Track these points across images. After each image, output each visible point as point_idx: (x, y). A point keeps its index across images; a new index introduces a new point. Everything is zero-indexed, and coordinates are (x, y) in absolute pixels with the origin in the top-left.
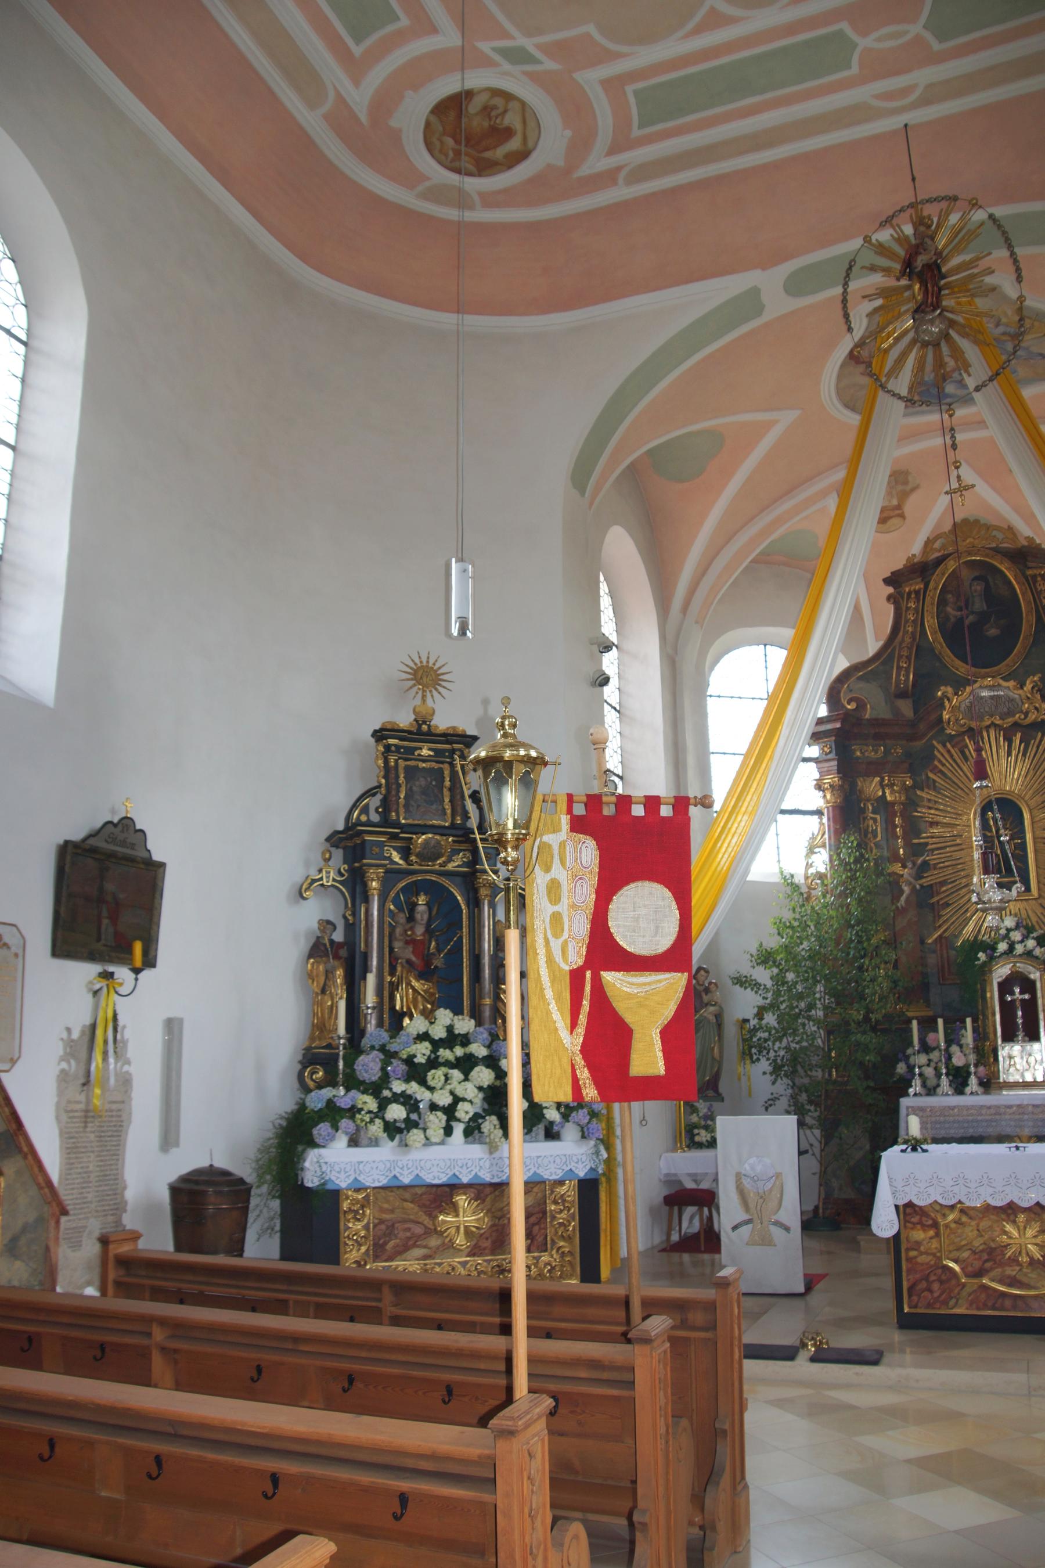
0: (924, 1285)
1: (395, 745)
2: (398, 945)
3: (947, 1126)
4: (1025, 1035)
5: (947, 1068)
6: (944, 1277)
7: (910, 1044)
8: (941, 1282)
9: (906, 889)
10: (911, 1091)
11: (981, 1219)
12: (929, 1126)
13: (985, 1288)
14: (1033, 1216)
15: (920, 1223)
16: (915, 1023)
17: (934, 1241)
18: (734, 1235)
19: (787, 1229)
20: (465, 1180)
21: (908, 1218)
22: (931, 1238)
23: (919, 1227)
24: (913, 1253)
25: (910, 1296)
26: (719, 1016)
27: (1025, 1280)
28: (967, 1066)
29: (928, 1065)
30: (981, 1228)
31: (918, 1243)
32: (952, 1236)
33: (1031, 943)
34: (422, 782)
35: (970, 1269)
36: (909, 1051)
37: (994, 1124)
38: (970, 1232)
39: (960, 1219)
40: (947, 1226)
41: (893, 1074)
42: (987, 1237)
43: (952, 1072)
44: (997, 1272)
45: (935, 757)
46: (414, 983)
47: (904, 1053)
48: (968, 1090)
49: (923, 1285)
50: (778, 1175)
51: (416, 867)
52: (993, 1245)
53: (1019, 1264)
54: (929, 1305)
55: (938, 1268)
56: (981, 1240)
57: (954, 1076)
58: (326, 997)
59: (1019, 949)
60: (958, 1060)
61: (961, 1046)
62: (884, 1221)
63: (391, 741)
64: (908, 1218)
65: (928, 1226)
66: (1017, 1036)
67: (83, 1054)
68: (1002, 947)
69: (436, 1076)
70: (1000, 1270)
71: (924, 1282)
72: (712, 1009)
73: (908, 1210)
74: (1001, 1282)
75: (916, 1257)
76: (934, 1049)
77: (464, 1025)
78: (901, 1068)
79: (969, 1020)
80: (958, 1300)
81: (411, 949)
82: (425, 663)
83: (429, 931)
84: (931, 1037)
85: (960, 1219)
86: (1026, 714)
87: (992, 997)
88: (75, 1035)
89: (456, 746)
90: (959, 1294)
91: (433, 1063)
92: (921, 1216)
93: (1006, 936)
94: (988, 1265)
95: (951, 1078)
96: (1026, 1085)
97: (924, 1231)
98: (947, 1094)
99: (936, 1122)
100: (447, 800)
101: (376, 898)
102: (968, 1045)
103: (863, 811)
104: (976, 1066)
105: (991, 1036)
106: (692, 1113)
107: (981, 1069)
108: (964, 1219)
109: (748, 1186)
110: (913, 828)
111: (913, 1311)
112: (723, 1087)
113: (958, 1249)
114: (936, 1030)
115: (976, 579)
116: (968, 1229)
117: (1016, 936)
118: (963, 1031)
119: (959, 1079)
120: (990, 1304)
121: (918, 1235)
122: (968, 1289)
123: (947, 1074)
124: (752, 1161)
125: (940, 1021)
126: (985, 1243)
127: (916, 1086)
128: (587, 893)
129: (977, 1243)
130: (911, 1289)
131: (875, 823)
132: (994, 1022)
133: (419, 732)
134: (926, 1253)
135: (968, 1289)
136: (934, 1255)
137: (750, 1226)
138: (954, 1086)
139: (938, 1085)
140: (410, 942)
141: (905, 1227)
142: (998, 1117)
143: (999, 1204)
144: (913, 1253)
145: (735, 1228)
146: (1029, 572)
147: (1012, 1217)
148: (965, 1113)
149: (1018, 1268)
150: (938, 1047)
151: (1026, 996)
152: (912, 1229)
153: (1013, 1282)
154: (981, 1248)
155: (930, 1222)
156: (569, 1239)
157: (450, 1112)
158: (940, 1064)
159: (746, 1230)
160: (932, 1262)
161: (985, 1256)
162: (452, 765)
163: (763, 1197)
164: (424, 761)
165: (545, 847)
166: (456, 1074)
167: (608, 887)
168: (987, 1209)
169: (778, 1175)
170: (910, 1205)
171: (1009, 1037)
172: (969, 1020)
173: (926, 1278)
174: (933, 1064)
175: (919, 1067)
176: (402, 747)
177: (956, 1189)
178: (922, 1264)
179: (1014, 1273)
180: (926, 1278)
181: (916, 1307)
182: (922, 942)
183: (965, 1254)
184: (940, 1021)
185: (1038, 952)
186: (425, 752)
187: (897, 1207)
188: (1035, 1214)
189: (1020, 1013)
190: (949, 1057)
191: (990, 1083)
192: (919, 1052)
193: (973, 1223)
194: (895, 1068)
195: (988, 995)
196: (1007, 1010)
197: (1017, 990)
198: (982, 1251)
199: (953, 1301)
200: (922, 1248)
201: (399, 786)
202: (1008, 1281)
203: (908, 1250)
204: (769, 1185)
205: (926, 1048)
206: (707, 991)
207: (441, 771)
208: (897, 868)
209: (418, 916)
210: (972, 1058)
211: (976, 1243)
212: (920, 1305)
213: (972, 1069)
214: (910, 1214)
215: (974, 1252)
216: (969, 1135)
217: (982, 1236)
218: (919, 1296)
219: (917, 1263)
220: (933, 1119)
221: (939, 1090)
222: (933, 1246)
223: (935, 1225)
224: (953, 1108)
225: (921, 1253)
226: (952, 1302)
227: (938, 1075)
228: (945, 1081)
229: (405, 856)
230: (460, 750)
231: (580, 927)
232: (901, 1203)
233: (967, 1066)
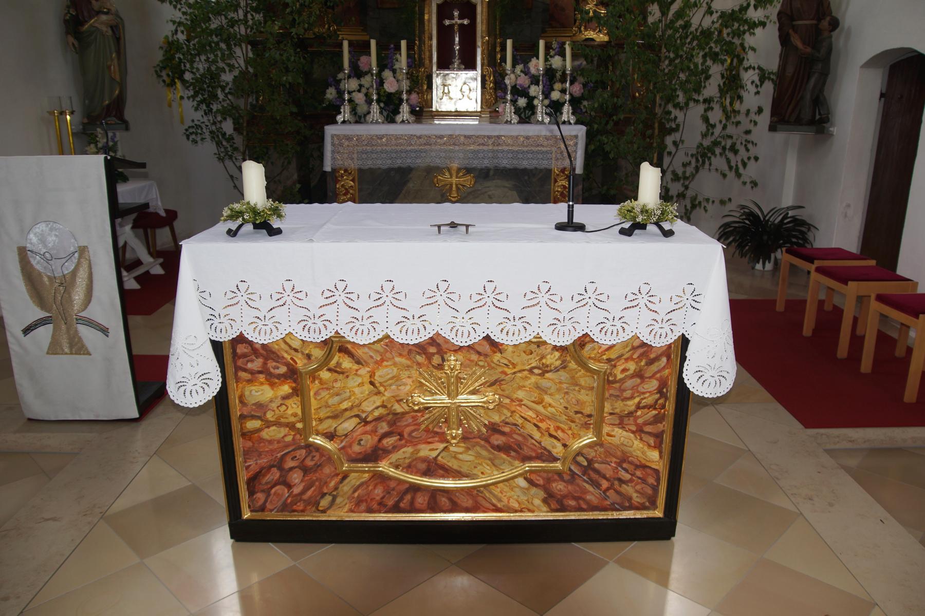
0: (275, 474)
3: (374, 156)
4: (461, 63)
5: (378, 94)
6: (309, 463)
7: (341, 69)
8: (306, 470)
10: (340, 118)
11: (379, 363)
12: (355, 156)
13: (382, 478)
14: (474, 357)
15: (264, 371)
16: (346, 44)
17: (289, 402)
18: (27, 340)
19: (105, 331)
21: (240, 362)
22: (286, 397)
23: (262, 377)
24: (252, 425)
25: (251, 493)
26: (117, 30)
27: (453, 464)
28: (399, 93)
29: (359, 91)
30: (377, 379)
31: (261, 407)
32: (324, 394)
35: (356, 448)
36: (340, 76)
37: (423, 155)
38: (356, 386)
39: (338, 364)
40: (313, 375)
41: (322, 101)
42: (388, 394)
43: (384, 99)
47: (335, 77)
48: (399, 118)
49: (275, 474)
50: (83, 250)
52: (398, 408)
53: (443, 438)
54: (285, 507)
55: (300, 448)
56: (378, 401)
57: (386, 104)
60: (390, 86)
61: (394, 71)
62: (192, 377)
64: (240, 362)
65: (279, 376)
66: (453, 63)
70: (409, 450)
71: (274, 470)
72: (104, 18)
73: (241, 349)
74: (409, 468)
75: (259, 430)
76: (366, 73)
78: (331, 93)
79: (403, 43)
80: (334, 498)
84: (364, 59)
85: (338, 364)
87: (430, 21)
90: (336, 488)
92: (266, 359)
94: (389, 442)
95: (382, 105)
96: (458, 114)
97: (272, 385)
98: (377, 122)
99: (363, 152)
102: (401, 69)
105: (427, 62)
106: (90, 143)
107: (414, 97)
108: (347, 363)
109: (38, 267)
111: (259, 516)
112: (128, 114)
113: (335, 417)
114: (369, 54)
116: (353, 382)
118: (398, 56)
119: (390, 106)
120: (390, 503)
121: (261, 392)
122: (354, 480)
123: (378, 101)
124: (42, 227)
125: (373, 43)
126: (383, 406)
127: (345, 113)
129: (371, 406)
130: (252, 482)
132: (431, 46)
134: (277, 423)
135: (354, 480)
136: (291, 426)
137: (50, 327)
138: (385, 113)
139: (369, 113)
141: (238, 379)
142: (427, 147)
143: (413, 339)
144: (252, 425)
145: (27, 331)
147: (436, 360)
148: (394, 142)
149: (442, 446)
150: (369, 72)
151: (466, 22)
152: (249, 381)
153: (433, 468)
154: (376, 414)
155: (283, 370)
158: (371, 90)
159: (44, 333)
160: (289, 439)
161: (384, 427)
163: (67, 283)
169: (83, 250)
170: (241, 339)
171: (445, 64)
172: (403, 43)
173: (279, 464)
174: (364, 90)
175: (349, 93)
177: (330, 313)
178: (270, 442)
179: (434, 454)
180: (279, 464)
181: (262, 509)
183: (348, 425)
184: (373, 43)
187: (217, 346)
188: (479, 353)
189: (457, 39)
190: (381, 83)
191: (423, 112)
192: (349, 77)
193: (364, 371)
194: (324, 93)
195: (426, 17)
196: (445, 34)
197: (456, 14)
198: (378, 419)
199: (328, 499)
200: (269, 416)
202: (423, 466)
203: (243, 417)
204: (70, 266)
205: (357, 73)
210: (405, 85)
211: (368, 406)
212: (269, 506)
213: (405, 97)
214: (244, 356)
215: (365, 422)
216: (396, 166)
217: (379, 393)
218: (267, 492)
219: (261, 440)
220: (360, 149)
221: (369, 118)
222: (290, 412)
223: (293, 374)
224: (380, 137)
225: (268, 424)
226: (324, 503)
227: (369, 101)
228: (375, 108)
232: (225, 337)
233: (399, 93)
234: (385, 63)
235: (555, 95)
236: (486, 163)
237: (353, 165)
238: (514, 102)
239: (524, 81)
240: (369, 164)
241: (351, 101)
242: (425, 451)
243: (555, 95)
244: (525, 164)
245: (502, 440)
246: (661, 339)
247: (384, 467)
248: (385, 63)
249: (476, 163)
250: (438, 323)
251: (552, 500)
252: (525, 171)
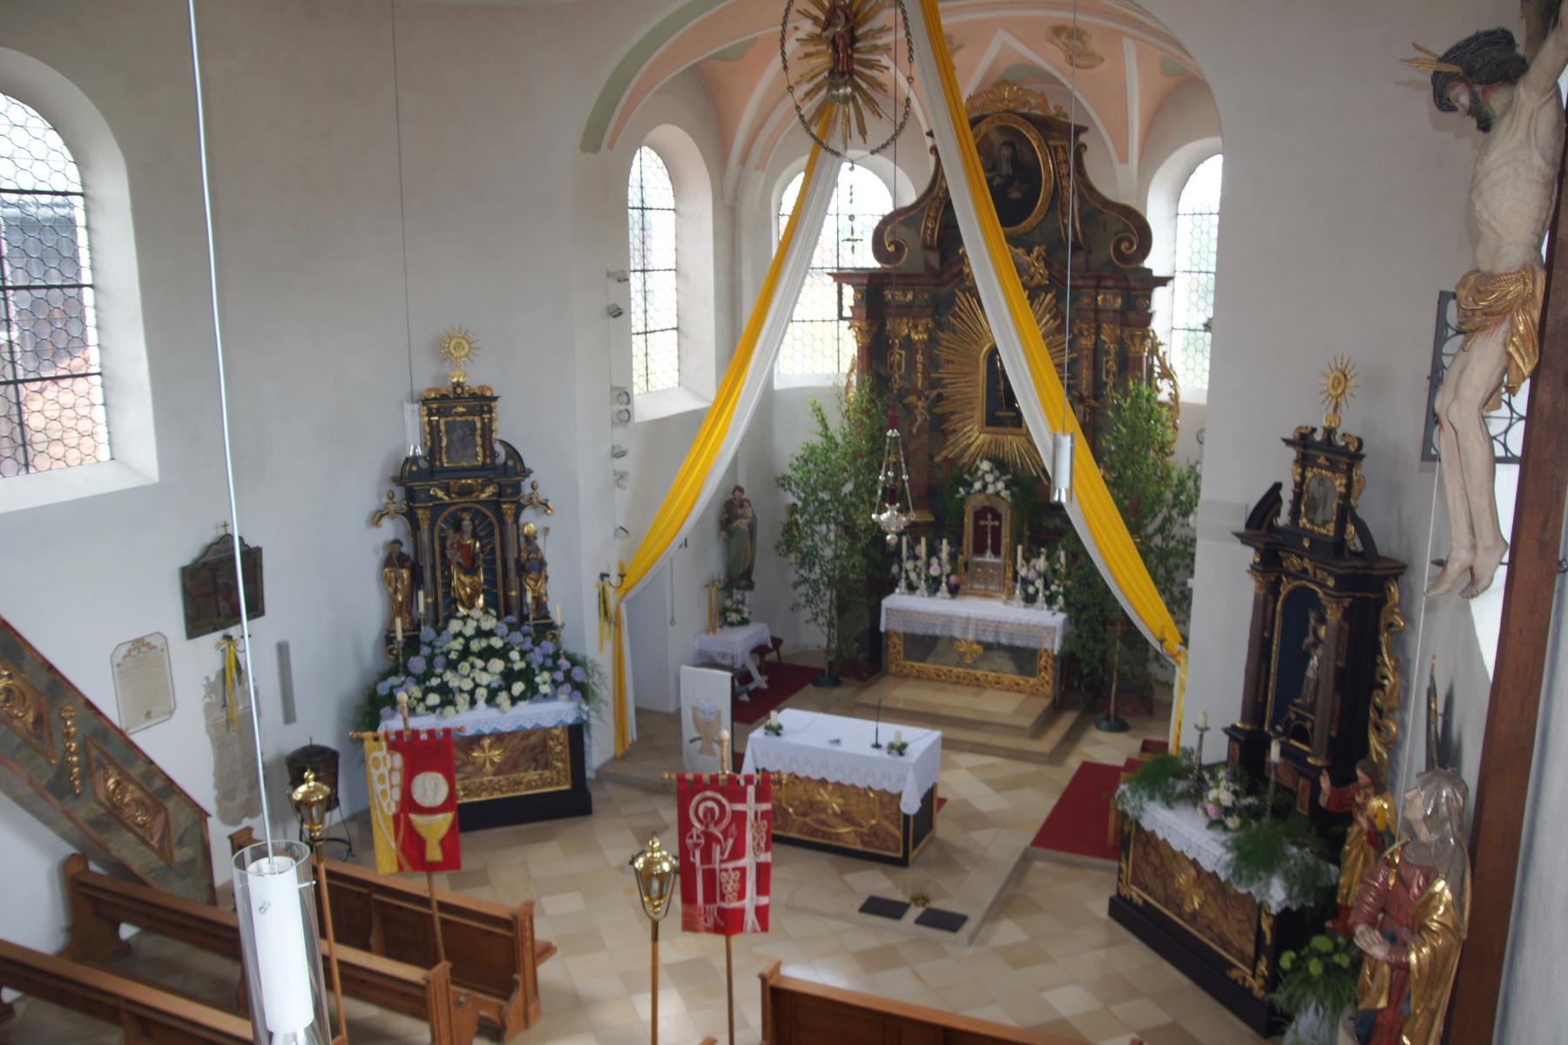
2: (449, 554)
9: (919, 419)
20: (487, 731)
33: (1000, 485)
34: (460, 433)
38: (800, 789)
44: (814, 816)
45: (954, 303)
59: (991, 489)
60: (934, 571)
67: (220, 689)
68: (978, 485)
69: (464, 667)
77: (489, 623)
78: (895, 569)
86: (1032, 278)
88: (212, 679)
91: (465, 653)
93: (983, 477)
103: (892, 347)
104: (948, 576)
107: (953, 579)
110: (933, 363)
112: (754, 577)
115: (1004, 144)
117: (990, 478)
119: (934, 585)
125: (923, 540)
128: (397, 778)
129: (804, 798)
131: (898, 356)
146: (1051, 143)
156: (563, 761)
157: (472, 693)
159: (698, 744)
165: (375, 759)
166: (479, 663)
167: (410, 773)
168: (808, 779)
182: (931, 458)
185: (1004, 493)
186: (461, 409)
190: (928, 565)
196: (979, 532)
206: (742, 506)
208: (912, 399)
210: (947, 568)
229: (448, 494)
231: (396, 794)
234: (933, 551)
235: (1053, 588)
236: (990, 639)
237: (900, 629)
238: (1025, 590)
239: (1032, 575)
240: (909, 630)
241: (908, 577)
242: (823, 816)
243: (1053, 588)
244: (1018, 643)
245: (846, 817)
246: (894, 791)
247: (808, 820)
248: (933, 551)
249: (983, 638)
250: (824, 774)
251: (863, 843)
252: (1018, 648)
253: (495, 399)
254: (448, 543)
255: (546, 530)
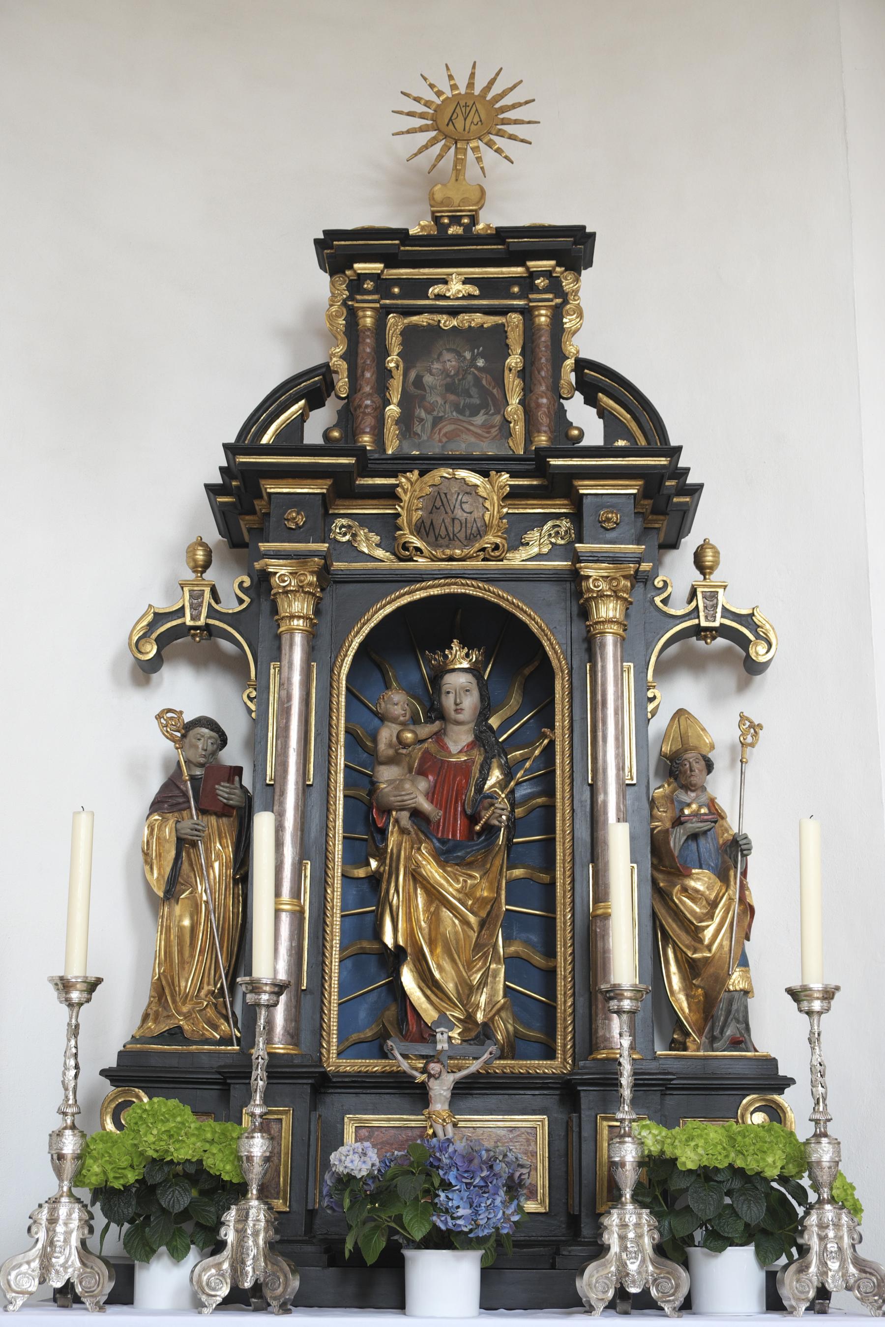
1: (376, 277)
46: (432, 871)
51: (421, 562)
58: (178, 909)
63: (361, 267)
81: (423, 784)
82: (463, 90)
83: (484, 737)
89: (536, 265)
100: (514, 401)
101: (298, 638)
133: (441, 238)
140: (430, 765)
162: (527, 313)
164: (453, 312)
176: (398, 282)
186: (456, 288)
201: (384, 374)
207: (500, 331)
209: (449, 702)
230: (548, 274)
253: (572, 247)
254: (386, 734)
255: (751, 729)
